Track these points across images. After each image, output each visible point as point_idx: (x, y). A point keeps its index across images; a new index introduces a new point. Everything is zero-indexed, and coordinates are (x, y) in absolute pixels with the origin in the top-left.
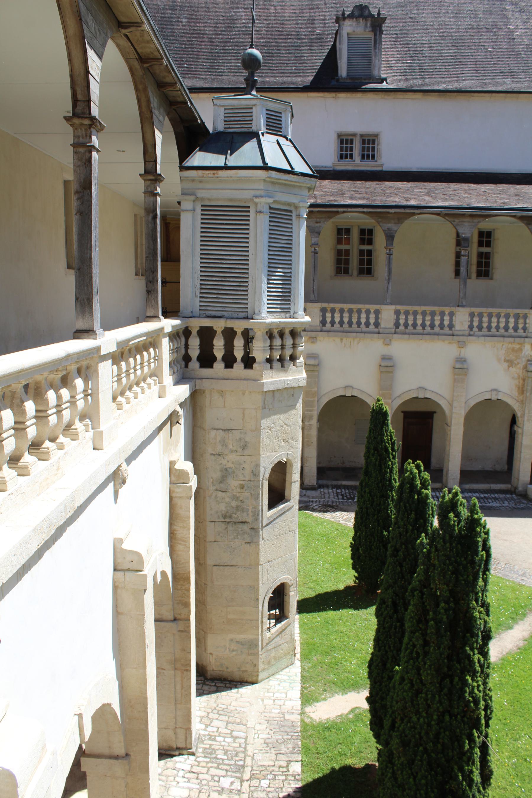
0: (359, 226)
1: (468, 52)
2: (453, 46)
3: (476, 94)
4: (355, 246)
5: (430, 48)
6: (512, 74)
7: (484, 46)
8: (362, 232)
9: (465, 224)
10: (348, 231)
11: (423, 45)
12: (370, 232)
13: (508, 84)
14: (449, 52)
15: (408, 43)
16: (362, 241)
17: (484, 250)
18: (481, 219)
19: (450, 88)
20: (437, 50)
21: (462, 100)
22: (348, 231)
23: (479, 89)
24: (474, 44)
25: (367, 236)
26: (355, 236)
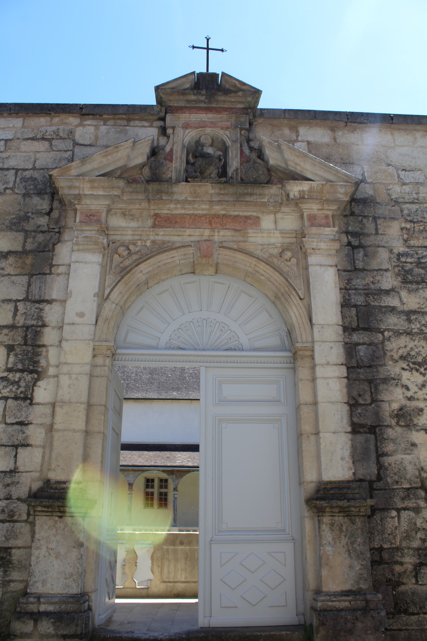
0: (159, 478)
1: (156, 377)
2: (149, 373)
3: (155, 400)
4: (156, 490)
5: (136, 374)
6: (178, 389)
7: (167, 374)
8: (161, 480)
9: (131, 475)
10: (153, 480)
11: (132, 373)
12: (166, 481)
13: (175, 394)
14: (145, 377)
15: (124, 372)
16: (161, 487)
17: (163, 490)
18: (140, 472)
19: (140, 397)
20: (140, 376)
21: (147, 403)
22: (153, 480)
23: (156, 397)
24: (161, 372)
25: (164, 483)
26: (156, 483)
